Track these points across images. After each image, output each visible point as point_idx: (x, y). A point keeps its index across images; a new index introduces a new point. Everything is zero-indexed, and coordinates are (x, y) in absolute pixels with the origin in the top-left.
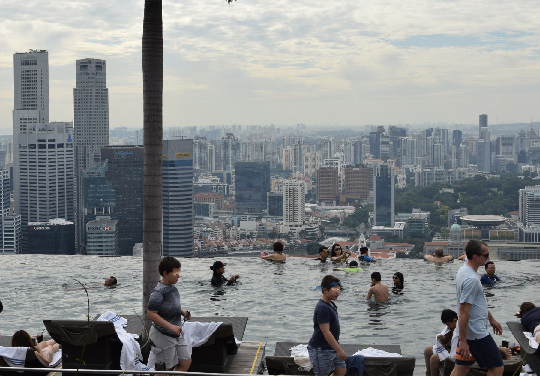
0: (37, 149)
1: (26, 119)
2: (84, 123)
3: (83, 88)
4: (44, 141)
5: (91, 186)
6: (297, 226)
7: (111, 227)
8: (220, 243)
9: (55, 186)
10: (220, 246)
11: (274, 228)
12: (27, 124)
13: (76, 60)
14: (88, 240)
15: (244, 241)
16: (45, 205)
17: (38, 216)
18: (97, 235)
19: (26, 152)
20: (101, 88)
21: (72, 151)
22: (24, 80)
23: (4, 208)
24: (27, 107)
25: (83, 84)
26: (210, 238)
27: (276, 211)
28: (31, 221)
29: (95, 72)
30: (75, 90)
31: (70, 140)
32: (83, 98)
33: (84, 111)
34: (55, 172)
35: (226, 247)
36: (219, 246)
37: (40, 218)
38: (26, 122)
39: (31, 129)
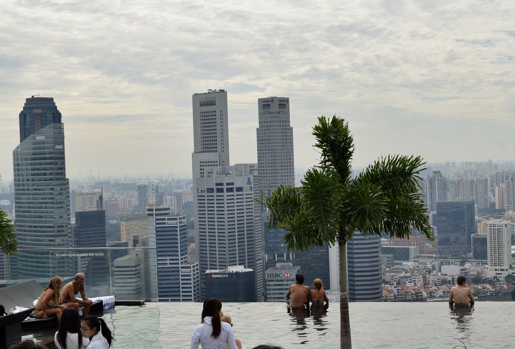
0: (215, 194)
1: (206, 162)
2: (268, 165)
3: (266, 128)
4: (222, 184)
5: (271, 231)
6: (503, 270)
7: (291, 273)
8: (418, 290)
9: (235, 232)
10: (417, 293)
11: (478, 272)
12: (205, 168)
13: (260, 100)
14: (268, 287)
15: (444, 287)
16: (225, 251)
17: (218, 263)
18: (277, 283)
19: (204, 196)
20: (284, 127)
21: (251, 194)
22: (204, 122)
23: (181, 255)
24: (207, 150)
25: (266, 124)
26: (408, 285)
27: (481, 255)
28: (211, 269)
29: (278, 110)
30: (258, 130)
31: (249, 183)
32: (267, 138)
33: (267, 152)
34: (234, 217)
35: (425, 294)
36: (416, 293)
37: (219, 265)
38: (204, 166)
39: (209, 173)
